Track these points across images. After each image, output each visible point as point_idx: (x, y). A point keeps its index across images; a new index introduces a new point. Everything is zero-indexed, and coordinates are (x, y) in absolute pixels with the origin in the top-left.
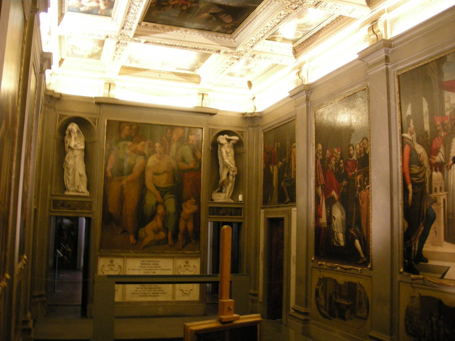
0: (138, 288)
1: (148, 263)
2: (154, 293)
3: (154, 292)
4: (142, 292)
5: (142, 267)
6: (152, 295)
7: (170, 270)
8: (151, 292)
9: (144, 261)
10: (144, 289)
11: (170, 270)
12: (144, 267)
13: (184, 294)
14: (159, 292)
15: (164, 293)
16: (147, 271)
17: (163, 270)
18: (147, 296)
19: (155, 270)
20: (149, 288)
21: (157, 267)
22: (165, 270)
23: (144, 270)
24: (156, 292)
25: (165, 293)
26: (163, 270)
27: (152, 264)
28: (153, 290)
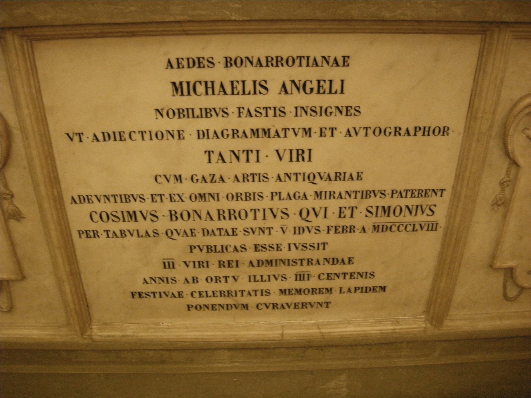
0: (169, 264)
1: (235, 73)
2: (299, 291)
3: (292, 284)
4: (202, 286)
5: (181, 113)
6: (276, 298)
7: (444, 131)
8: (274, 286)
9: (198, 63)
10: (214, 271)
11: (444, 131)
12: (207, 113)
13: (512, 292)
14: (336, 283)
15: (373, 290)
16: (239, 145)
17: (382, 131)
18: (246, 307)
19: (308, 132)
20: (260, 263)
21: (326, 112)
22: (397, 131)
23: (202, 134)
24: (313, 283)
25: (383, 289)
26: (382, 131)
27: (275, 87)
28: (290, 271)
